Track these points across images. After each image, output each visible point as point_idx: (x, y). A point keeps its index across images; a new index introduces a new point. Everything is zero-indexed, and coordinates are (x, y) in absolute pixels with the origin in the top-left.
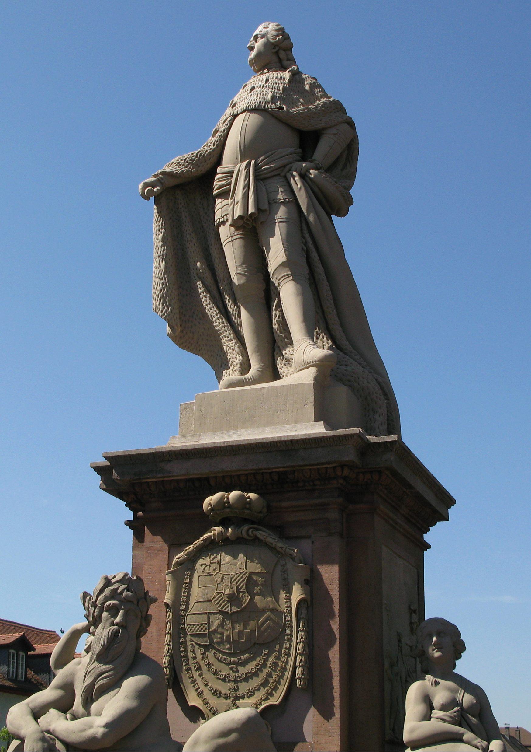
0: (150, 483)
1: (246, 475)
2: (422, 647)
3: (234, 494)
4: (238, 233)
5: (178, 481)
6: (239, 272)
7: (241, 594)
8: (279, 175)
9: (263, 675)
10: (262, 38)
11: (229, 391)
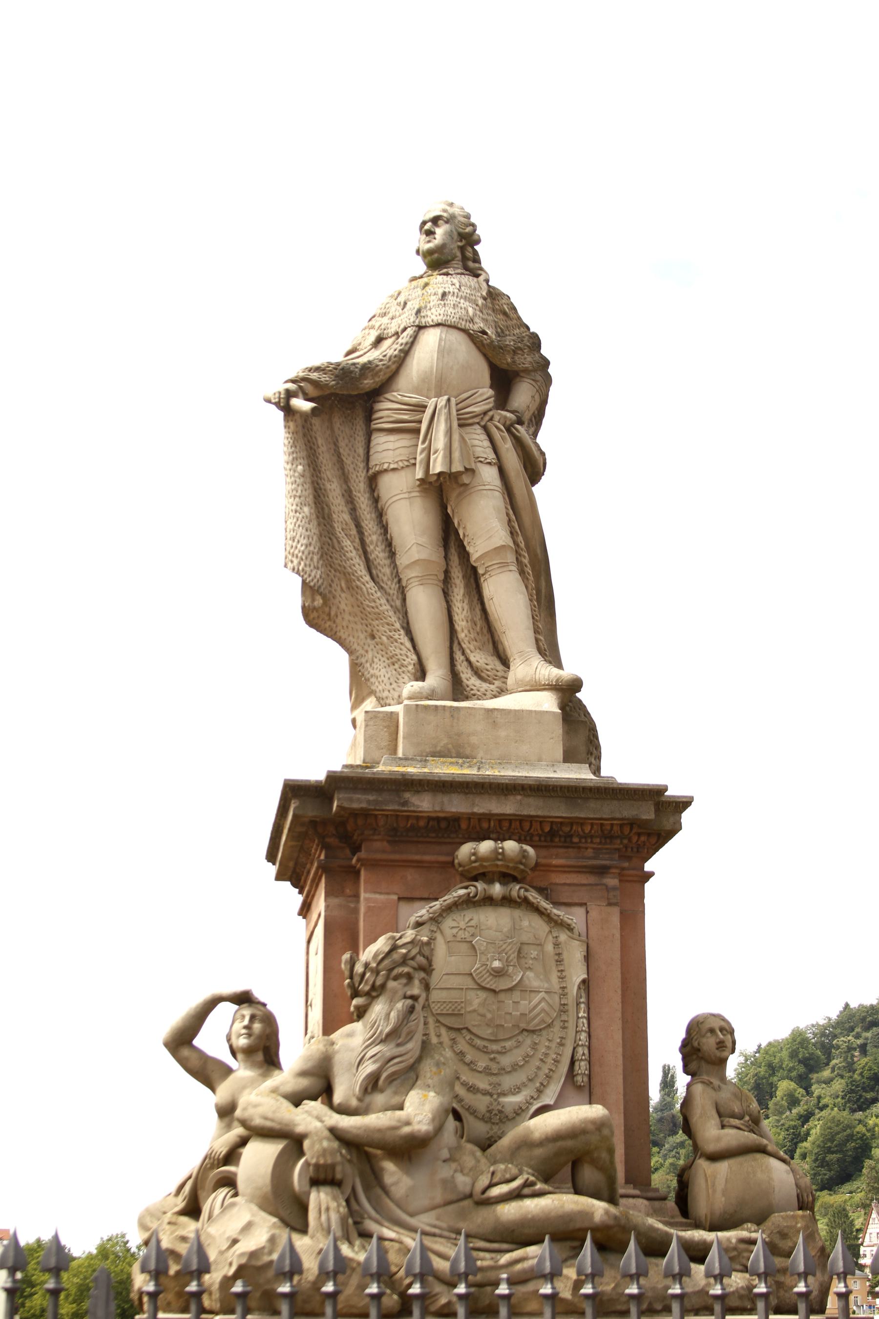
0: (380, 817)
1: (510, 821)
2: (699, 1044)
3: (511, 846)
4: (418, 489)
5: (418, 818)
6: (419, 542)
7: (511, 968)
8: (478, 423)
9: (530, 1070)
10: (447, 222)
11: (444, 706)
